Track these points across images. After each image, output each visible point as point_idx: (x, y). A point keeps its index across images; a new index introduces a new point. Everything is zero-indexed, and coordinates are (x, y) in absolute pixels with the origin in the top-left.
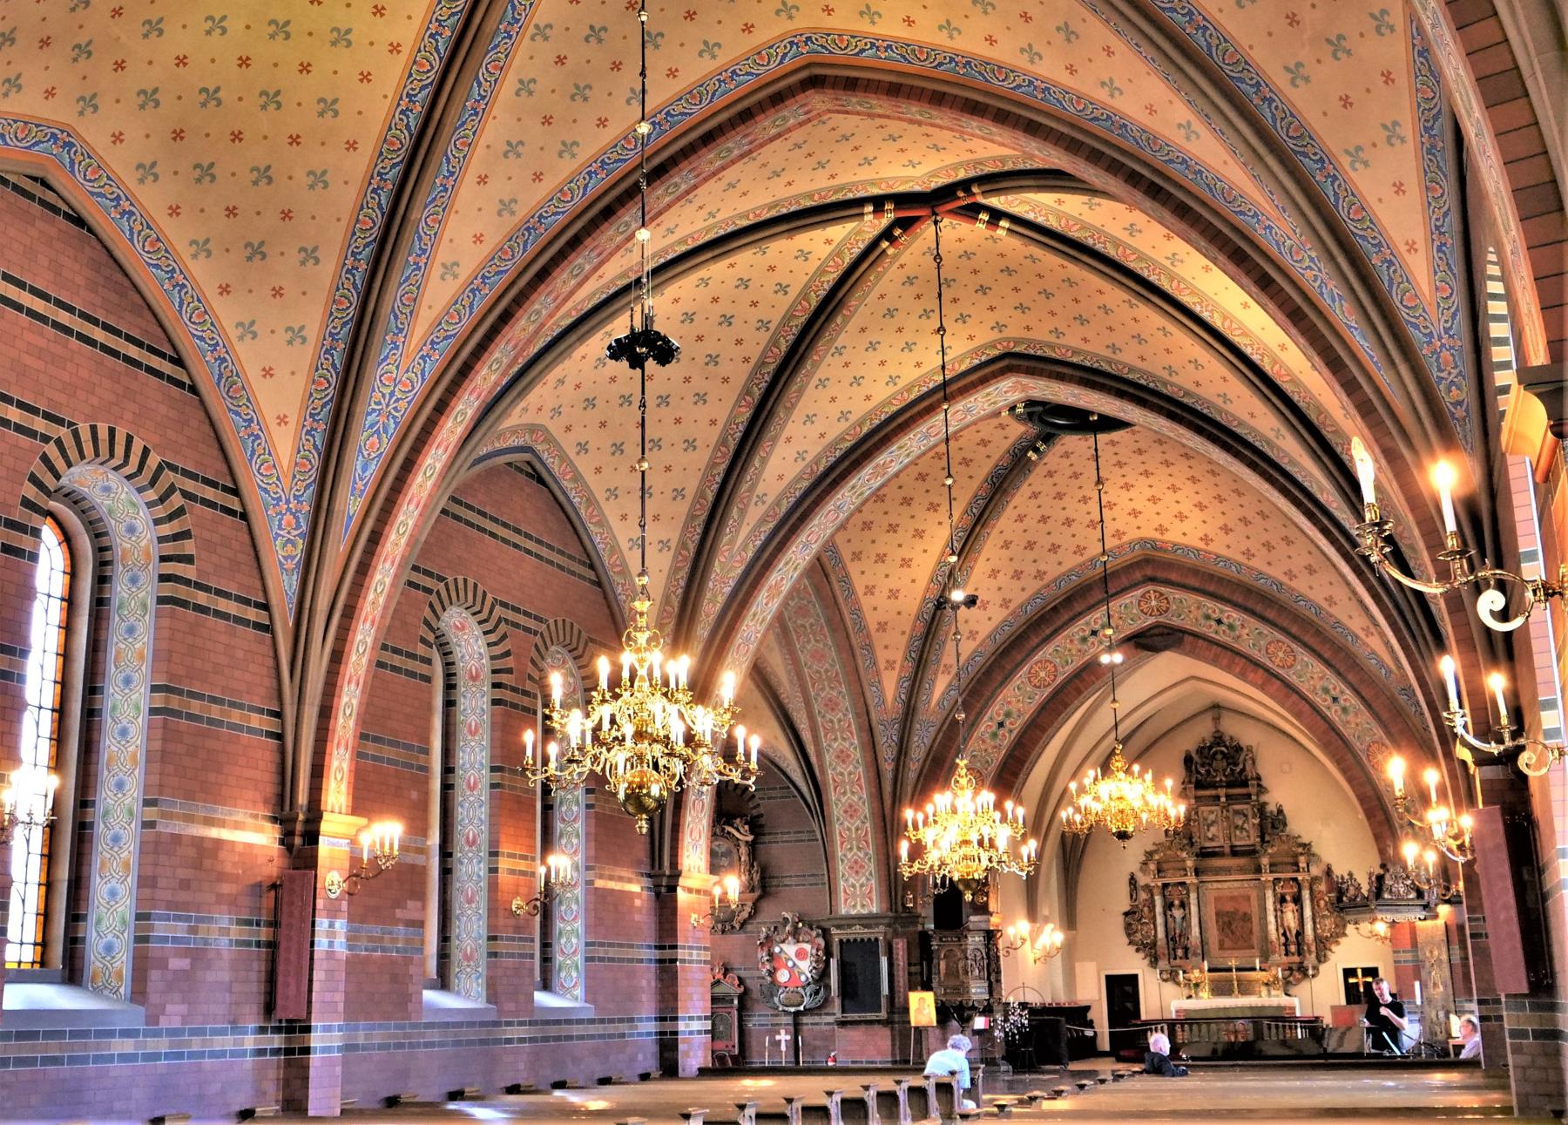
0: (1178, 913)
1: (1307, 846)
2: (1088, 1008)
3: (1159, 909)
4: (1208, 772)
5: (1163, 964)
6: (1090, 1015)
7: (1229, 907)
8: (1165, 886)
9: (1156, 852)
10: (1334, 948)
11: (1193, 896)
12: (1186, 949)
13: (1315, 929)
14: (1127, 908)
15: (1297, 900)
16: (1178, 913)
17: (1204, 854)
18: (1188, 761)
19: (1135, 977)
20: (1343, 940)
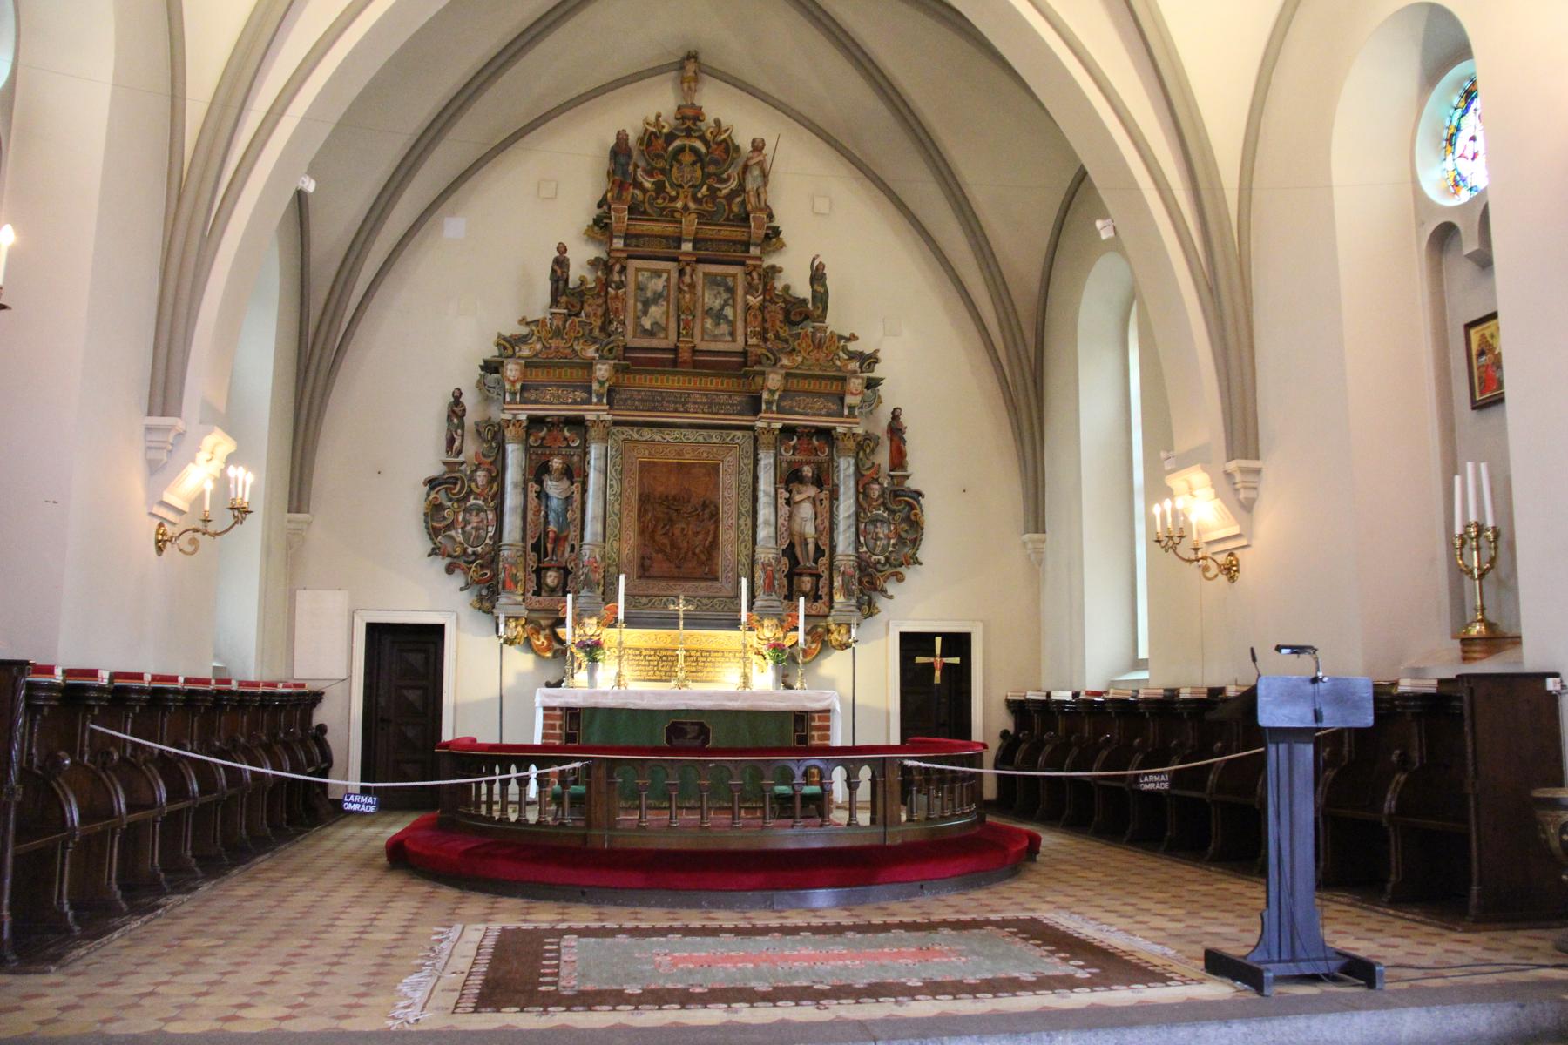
0: (555, 488)
1: (868, 360)
2: (316, 697)
3: (513, 474)
4: (660, 187)
5: (510, 602)
6: (320, 716)
7: (669, 485)
8: (535, 422)
10: (891, 587)
11: (595, 451)
12: (566, 572)
13: (858, 544)
14: (435, 469)
16: (555, 488)
17: (630, 362)
18: (620, 152)
19: (439, 630)
20: (909, 573)
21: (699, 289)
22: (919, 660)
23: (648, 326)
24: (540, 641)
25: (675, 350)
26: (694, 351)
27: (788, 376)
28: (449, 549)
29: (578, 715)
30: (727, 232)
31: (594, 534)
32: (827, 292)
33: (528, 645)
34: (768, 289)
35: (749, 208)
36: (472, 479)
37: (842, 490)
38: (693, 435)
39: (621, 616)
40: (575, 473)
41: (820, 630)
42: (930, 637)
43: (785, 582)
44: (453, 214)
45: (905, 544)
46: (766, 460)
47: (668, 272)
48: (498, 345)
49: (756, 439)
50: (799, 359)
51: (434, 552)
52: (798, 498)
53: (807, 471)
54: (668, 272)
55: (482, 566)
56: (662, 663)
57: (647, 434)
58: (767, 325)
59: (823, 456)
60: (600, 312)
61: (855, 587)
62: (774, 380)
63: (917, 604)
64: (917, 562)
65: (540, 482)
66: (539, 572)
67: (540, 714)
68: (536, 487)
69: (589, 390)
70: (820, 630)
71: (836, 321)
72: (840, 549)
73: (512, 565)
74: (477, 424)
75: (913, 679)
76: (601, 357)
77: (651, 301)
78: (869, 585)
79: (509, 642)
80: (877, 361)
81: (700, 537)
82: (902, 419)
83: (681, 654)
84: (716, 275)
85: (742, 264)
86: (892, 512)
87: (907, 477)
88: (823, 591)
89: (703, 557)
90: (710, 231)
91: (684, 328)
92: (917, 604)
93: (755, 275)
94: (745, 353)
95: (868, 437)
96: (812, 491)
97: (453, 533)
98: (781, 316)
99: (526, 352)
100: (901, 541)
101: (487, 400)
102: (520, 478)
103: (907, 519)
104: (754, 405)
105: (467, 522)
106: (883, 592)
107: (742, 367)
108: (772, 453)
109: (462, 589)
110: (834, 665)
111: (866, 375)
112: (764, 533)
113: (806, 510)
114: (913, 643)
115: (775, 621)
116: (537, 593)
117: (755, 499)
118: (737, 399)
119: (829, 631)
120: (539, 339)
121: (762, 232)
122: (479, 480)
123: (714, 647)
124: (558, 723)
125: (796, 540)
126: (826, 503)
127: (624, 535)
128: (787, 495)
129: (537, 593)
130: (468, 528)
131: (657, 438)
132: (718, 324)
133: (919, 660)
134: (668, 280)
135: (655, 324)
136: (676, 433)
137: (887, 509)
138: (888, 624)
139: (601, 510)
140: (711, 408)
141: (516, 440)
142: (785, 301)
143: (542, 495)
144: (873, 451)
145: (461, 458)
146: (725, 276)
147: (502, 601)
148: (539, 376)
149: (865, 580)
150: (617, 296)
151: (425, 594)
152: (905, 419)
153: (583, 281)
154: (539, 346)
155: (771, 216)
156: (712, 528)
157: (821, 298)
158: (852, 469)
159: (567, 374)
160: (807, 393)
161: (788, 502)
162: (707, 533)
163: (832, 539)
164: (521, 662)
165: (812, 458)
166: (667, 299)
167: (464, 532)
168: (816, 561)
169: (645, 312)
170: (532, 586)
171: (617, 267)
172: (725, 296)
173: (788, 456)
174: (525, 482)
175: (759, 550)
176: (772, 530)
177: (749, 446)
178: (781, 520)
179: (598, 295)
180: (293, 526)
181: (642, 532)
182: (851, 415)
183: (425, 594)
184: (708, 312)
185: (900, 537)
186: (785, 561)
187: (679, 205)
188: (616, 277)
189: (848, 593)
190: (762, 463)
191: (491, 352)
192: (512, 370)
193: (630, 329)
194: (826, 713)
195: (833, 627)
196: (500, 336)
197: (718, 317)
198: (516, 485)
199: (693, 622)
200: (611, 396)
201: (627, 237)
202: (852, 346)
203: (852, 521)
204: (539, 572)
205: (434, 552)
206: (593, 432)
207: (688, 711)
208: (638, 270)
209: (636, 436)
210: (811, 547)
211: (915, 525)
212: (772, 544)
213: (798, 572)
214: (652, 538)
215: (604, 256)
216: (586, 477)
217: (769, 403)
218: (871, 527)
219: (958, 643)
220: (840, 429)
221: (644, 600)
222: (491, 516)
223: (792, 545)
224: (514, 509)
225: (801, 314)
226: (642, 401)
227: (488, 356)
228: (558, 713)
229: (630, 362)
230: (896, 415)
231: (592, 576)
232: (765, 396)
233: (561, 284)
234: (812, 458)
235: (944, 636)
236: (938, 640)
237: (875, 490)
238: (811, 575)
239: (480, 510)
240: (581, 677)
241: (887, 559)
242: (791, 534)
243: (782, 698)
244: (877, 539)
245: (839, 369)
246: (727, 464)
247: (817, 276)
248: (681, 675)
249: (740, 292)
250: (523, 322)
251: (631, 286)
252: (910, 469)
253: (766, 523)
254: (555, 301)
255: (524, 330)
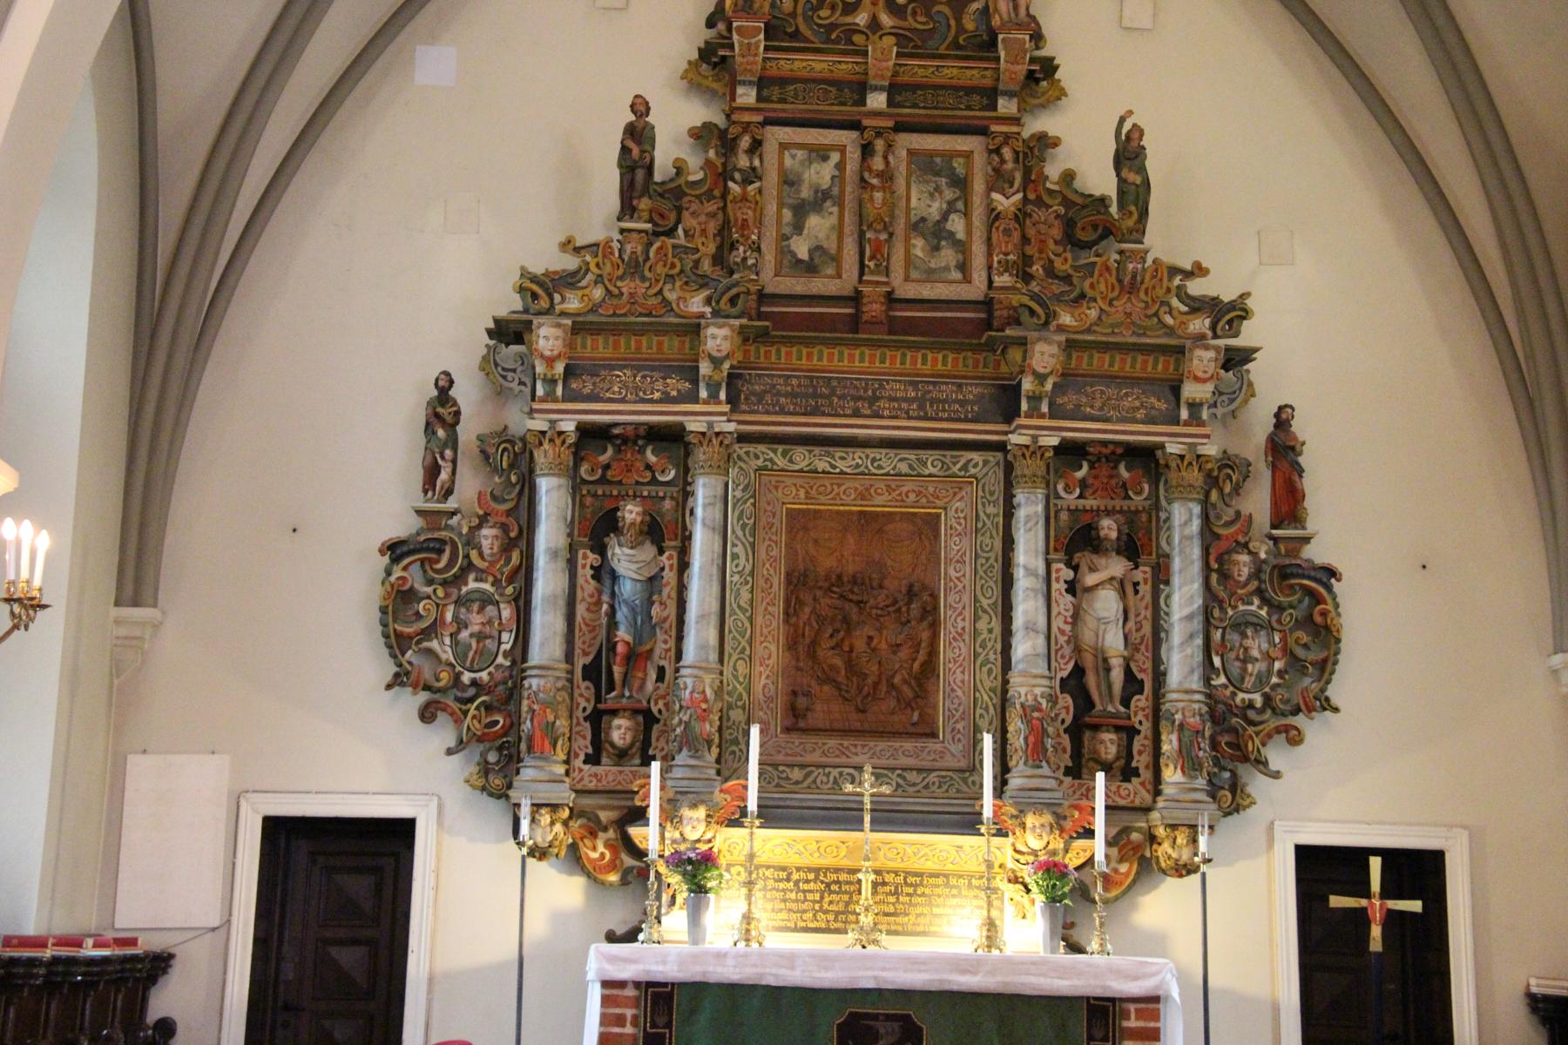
0: (628, 560)
1: (1230, 314)
2: (160, 963)
3: (549, 534)
5: (540, 778)
6: (164, 1001)
8: (591, 435)
9: (568, 280)
10: (1276, 755)
11: (704, 491)
12: (647, 719)
14: (403, 525)
15: (1139, 544)
17: (769, 322)
19: (403, 830)
20: (1313, 728)
21: (900, 182)
22: (1336, 901)
23: (803, 254)
24: (597, 851)
25: (856, 299)
26: (891, 299)
27: (1070, 346)
28: (427, 675)
29: (670, 996)
30: (952, 71)
31: (702, 647)
32: (1147, 184)
33: (575, 859)
34: (1032, 179)
35: (996, 21)
36: (471, 541)
37: (1177, 564)
38: (889, 461)
39: (752, 805)
40: (664, 532)
41: (1135, 836)
42: (1355, 858)
43: (1066, 741)
44: (433, 38)
45: (1303, 671)
46: (1030, 506)
47: (842, 149)
48: (521, 290)
49: (1009, 468)
50: (1093, 313)
51: (398, 681)
52: (1090, 579)
53: (1109, 528)
54: (842, 149)
55: (489, 708)
56: (828, 897)
57: (802, 457)
58: (1029, 250)
59: (1138, 500)
60: (712, 227)
61: (1204, 753)
62: (1045, 355)
63: (1332, 789)
64: (1328, 706)
65: (601, 550)
66: (598, 719)
67: (595, 994)
68: (593, 558)
69: (692, 375)
70: (1135, 836)
71: (1163, 241)
72: (1175, 677)
73: (546, 705)
74: (480, 438)
75: (1325, 941)
76: (716, 313)
77: (808, 209)
78: (1232, 751)
79: (539, 853)
80: (1245, 314)
81: (904, 653)
82: (1297, 426)
83: (867, 879)
84: (931, 154)
85: (983, 131)
86: (1278, 608)
87: (1307, 540)
88: (1141, 761)
89: (908, 692)
90: (920, 70)
91: (872, 256)
92: (1332, 789)
93: (1007, 153)
94: (987, 304)
95: (1228, 462)
96: (1116, 566)
97: (434, 644)
98: (1056, 232)
99: (573, 303)
100: (1296, 664)
101: (500, 393)
102: (562, 541)
103: (1307, 622)
104: (1007, 403)
105: (461, 624)
106: (1261, 763)
107: (983, 328)
108: (1040, 493)
109: (450, 752)
110: (1163, 907)
111: (1222, 342)
112: (1023, 647)
113: (1107, 603)
114: (1322, 869)
115: (1048, 818)
116: (593, 759)
117: (1007, 582)
118: (972, 391)
119: (1153, 839)
120: (599, 280)
121: (1022, 69)
122: (486, 544)
123: (929, 866)
124: (629, 1013)
125: (1088, 661)
126: (1145, 589)
127: (759, 650)
128: (1070, 574)
129: (593, 759)
130: (464, 634)
131: (821, 465)
132: (937, 248)
133: (1336, 901)
134: (841, 166)
135: (817, 249)
136: (858, 457)
137: (1265, 601)
138: (1270, 828)
139: (716, 605)
140: (925, 408)
141: (556, 469)
142: (1067, 203)
143: (604, 573)
144: (1237, 490)
145: (451, 504)
146: (950, 155)
147: (527, 773)
148: (597, 348)
149: (1224, 739)
150: (744, 198)
151: (378, 760)
152: (1300, 427)
153: (680, 168)
154: (598, 293)
155: (1038, 37)
156: (925, 636)
157: (1135, 195)
158: (1196, 525)
159: (648, 345)
160: (1109, 379)
161: (1072, 588)
162: (917, 647)
163: (1157, 660)
164: (559, 892)
165: (1118, 503)
166: (840, 204)
167: (455, 643)
168: (1126, 702)
169: (798, 228)
170: (584, 745)
171: (745, 142)
172: (949, 194)
173: (1071, 499)
174: (572, 549)
175: (1015, 679)
176: (1041, 641)
177: (995, 481)
178: (1057, 623)
179: (709, 195)
180: (123, 631)
181: (792, 645)
182: (1195, 419)
183: (378, 760)
184: (918, 226)
185: (1293, 659)
186: (1066, 700)
187: (861, 19)
188: (743, 161)
189: (1191, 766)
190: (1021, 514)
191: (509, 304)
192: (548, 337)
193: (769, 256)
194: (1151, 1003)
195: (1161, 832)
196: (524, 273)
197: (937, 234)
198: (554, 554)
199: (890, 818)
200: (735, 388)
201: (763, 83)
202: (1196, 287)
203: (1197, 624)
204: (598, 719)
205: (398, 681)
206: (700, 455)
207: (879, 992)
208: (784, 147)
209: (781, 462)
210: (1117, 676)
211: (1324, 634)
212: (1041, 668)
213: (1093, 726)
214: (812, 655)
215: (720, 120)
216: (687, 539)
217: (1035, 399)
218: (1234, 637)
219: (1419, 871)
220: (1173, 448)
221: (796, 774)
222: (507, 612)
223: (1079, 671)
224: (551, 600)
225: (1098, 226)
226: (794, 395)
227: (503, 312)
228: (630, 992)
229: (769, 322)
230: (1282, 419)
231: (696, 726)
232: (1027, 385)
233: (640, 174)
234: (1118, 503)
235: (1388, 855)
236: (1375, 863)
237: (1242, 565)
238: (1118, 729)
239: (486, 600)
240: (675, 922)
241: (1267, 699)
242: (1078, 650)
243: (1063, 972)
244: (1246, 660)
245: (1171, 331)
246: (955, 514)
247: (1129, 153)
248: (866, 920)
249: (978, 186)
250: (568, 245)
251: (772, 178)
252: (1312, 525)
253: (1030, 628)
254: (628, 208)
255: (570, 263)
